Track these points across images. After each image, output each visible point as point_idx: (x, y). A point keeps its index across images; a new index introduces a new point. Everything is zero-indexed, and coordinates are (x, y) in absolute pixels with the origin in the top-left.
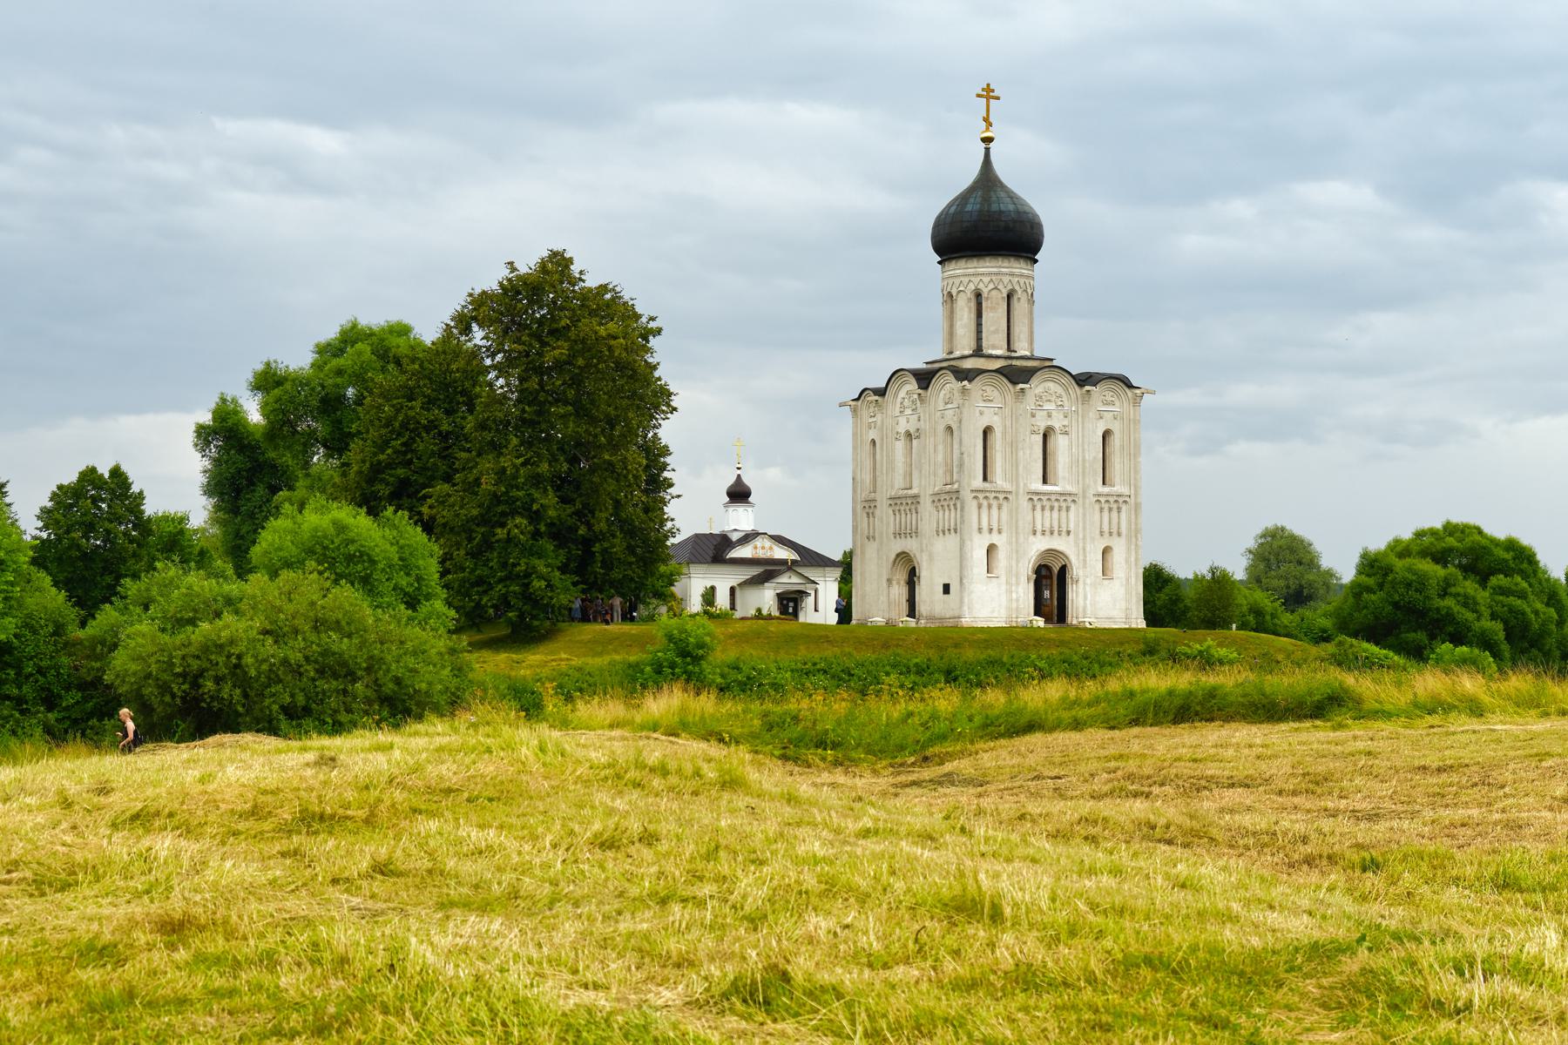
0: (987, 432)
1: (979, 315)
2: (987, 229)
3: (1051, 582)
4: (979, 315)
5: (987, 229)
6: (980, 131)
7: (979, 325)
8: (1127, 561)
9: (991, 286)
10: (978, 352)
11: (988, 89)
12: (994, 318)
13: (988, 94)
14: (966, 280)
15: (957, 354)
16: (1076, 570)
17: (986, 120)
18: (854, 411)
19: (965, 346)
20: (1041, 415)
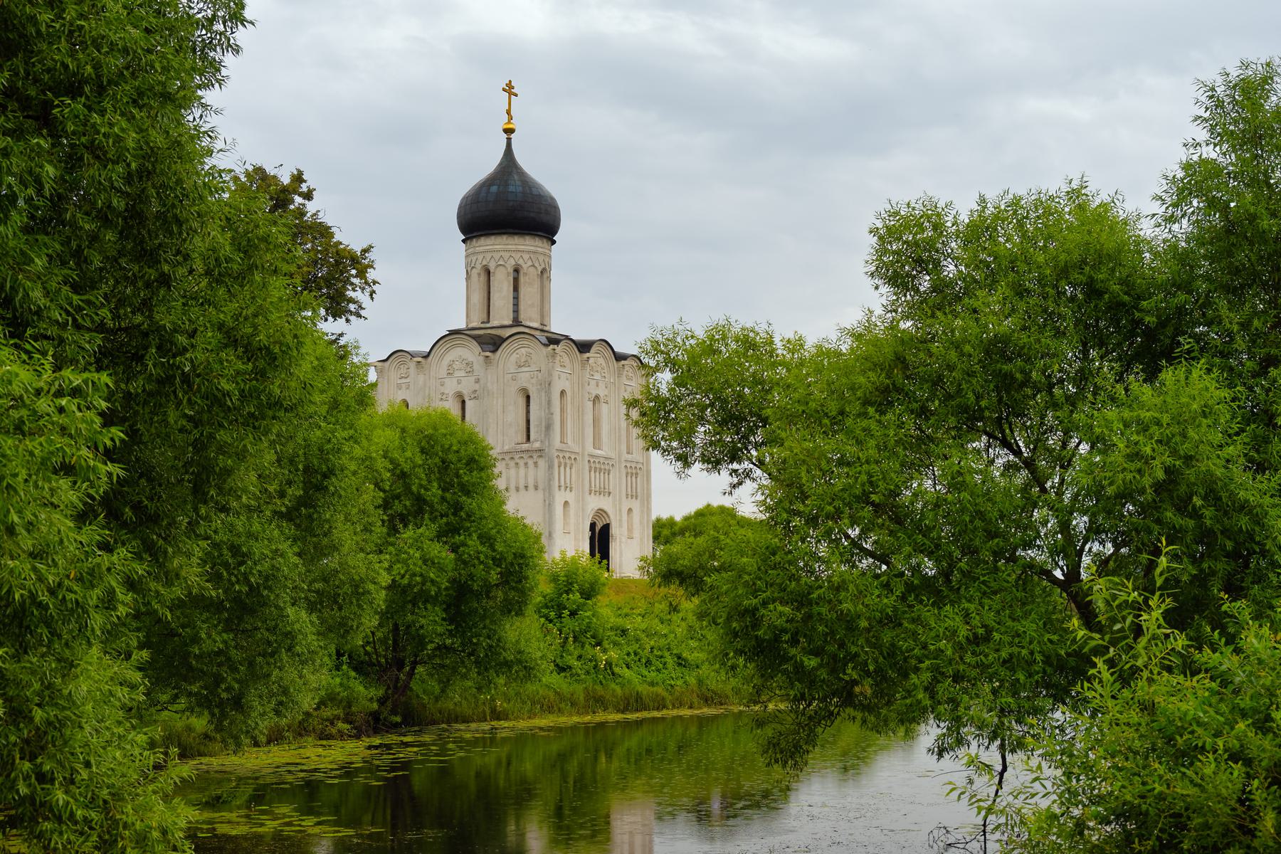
0: (563, 393)
1: (516, 289)
2: (508, 211)
3: (601, 540)
4: (516, 289)
5: (508, 211)
7: (516, 298)
8: (641, 523)
9: (530, 263)
10: (517, 322)
12: (529, 292)
13: (509, 89)
14: (506, 255)
15: (494, 323)
16: (614, 531)
17: (508, 112)
19: (502, 315)
20: (592, 383)
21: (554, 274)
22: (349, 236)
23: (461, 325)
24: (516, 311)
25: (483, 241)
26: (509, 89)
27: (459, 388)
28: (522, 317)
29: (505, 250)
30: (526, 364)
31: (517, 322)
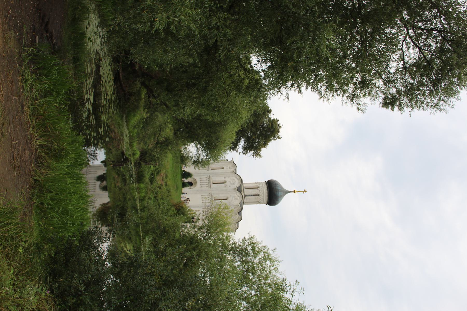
1: (254, 195)
4: (254, 195)
6: (296, 190)
7: (252, 195)
10: (246, 196)
11: (306, 191)
13: (305, 191)
14: (262, 192)
18: (230, 162)
19: (247, 192)
21: (258, 205)
22: (264, 151)
23: (244, 182)
24: (248, 196)
25: (266, 186)
26: (305, 191)
27: (227, 182)
28: (247, 197)
29: (264, 192)
30: (235, 199)
31: (246, 196)
